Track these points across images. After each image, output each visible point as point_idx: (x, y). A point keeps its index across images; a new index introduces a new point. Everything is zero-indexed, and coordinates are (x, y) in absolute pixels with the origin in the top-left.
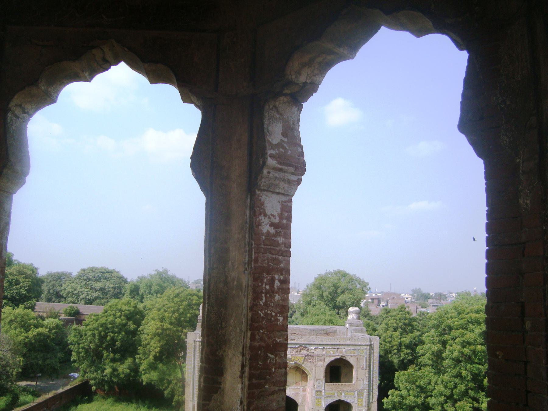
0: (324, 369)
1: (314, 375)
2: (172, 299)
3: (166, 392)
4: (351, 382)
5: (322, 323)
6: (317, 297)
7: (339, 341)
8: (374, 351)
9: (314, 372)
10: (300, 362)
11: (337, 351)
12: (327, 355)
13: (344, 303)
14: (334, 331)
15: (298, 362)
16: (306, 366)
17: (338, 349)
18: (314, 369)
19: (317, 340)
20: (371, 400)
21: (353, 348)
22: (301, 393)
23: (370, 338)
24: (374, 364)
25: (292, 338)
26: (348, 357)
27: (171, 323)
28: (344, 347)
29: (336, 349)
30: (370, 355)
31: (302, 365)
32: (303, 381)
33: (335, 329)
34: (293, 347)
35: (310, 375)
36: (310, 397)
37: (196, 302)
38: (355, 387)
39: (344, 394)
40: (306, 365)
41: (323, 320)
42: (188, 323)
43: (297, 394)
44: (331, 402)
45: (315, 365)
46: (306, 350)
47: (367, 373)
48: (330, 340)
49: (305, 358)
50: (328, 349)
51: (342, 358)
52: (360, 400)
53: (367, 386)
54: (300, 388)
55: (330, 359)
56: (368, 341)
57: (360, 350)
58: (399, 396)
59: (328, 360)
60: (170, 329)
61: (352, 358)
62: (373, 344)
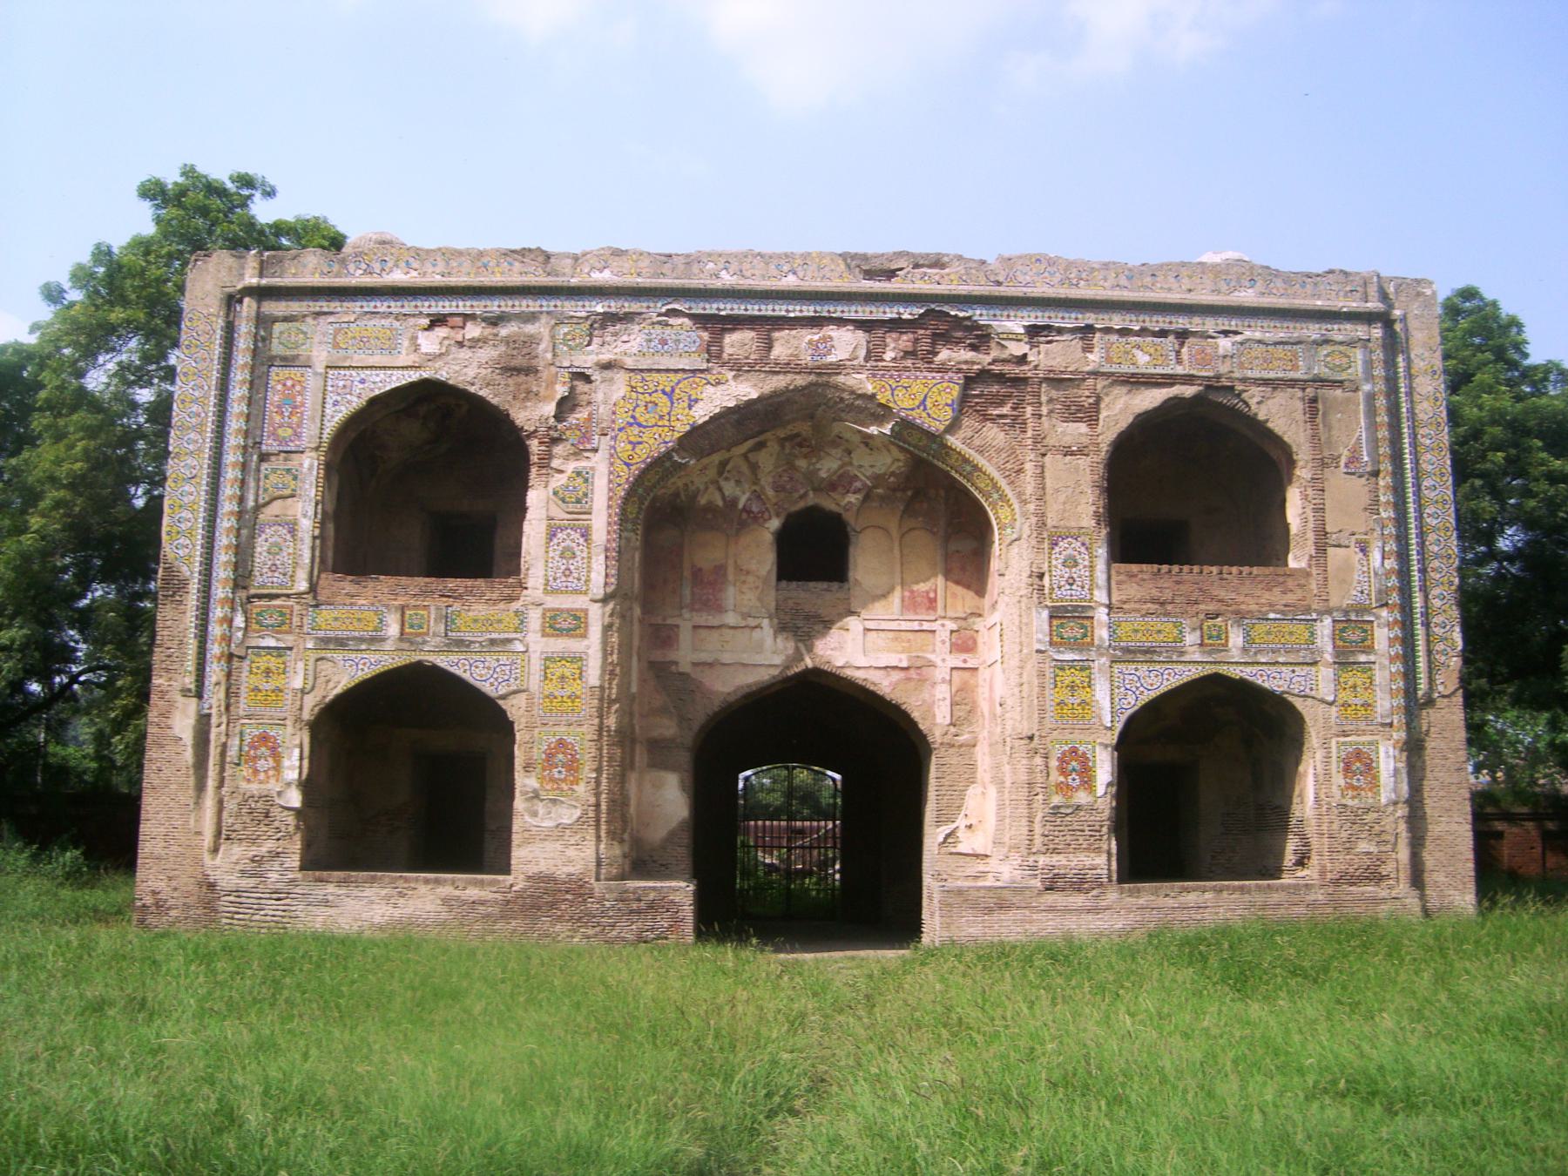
0: (1101, 469)
1: (1031, 507)
8: (1408, 361)
10: (936, 418)
11: (1178, 353)
12: (1113, 374)
17: (1182, 335)
18: (1029, 466)
20: (1423, 686)
21: (1281, 335)
22: (943, 660)
26: (1254, 390)
29: (1171, 338)
31: (953, 441)
34: (882, 323)
35: (1004, 513)
36: (1015, 662)
38: (1313, 586)
43: (917, 670)
44: (1163, 689)
45: (1038, 440)
47: (1385, 497)
48: (1129, 278)
49: (964, 398)
50: (1114, 338)
51: (1213, 397)
52: (1352, 678)
53: (1394, 581)
54: (935, 626)
56: (1373, 291)
61: (1281, 398)
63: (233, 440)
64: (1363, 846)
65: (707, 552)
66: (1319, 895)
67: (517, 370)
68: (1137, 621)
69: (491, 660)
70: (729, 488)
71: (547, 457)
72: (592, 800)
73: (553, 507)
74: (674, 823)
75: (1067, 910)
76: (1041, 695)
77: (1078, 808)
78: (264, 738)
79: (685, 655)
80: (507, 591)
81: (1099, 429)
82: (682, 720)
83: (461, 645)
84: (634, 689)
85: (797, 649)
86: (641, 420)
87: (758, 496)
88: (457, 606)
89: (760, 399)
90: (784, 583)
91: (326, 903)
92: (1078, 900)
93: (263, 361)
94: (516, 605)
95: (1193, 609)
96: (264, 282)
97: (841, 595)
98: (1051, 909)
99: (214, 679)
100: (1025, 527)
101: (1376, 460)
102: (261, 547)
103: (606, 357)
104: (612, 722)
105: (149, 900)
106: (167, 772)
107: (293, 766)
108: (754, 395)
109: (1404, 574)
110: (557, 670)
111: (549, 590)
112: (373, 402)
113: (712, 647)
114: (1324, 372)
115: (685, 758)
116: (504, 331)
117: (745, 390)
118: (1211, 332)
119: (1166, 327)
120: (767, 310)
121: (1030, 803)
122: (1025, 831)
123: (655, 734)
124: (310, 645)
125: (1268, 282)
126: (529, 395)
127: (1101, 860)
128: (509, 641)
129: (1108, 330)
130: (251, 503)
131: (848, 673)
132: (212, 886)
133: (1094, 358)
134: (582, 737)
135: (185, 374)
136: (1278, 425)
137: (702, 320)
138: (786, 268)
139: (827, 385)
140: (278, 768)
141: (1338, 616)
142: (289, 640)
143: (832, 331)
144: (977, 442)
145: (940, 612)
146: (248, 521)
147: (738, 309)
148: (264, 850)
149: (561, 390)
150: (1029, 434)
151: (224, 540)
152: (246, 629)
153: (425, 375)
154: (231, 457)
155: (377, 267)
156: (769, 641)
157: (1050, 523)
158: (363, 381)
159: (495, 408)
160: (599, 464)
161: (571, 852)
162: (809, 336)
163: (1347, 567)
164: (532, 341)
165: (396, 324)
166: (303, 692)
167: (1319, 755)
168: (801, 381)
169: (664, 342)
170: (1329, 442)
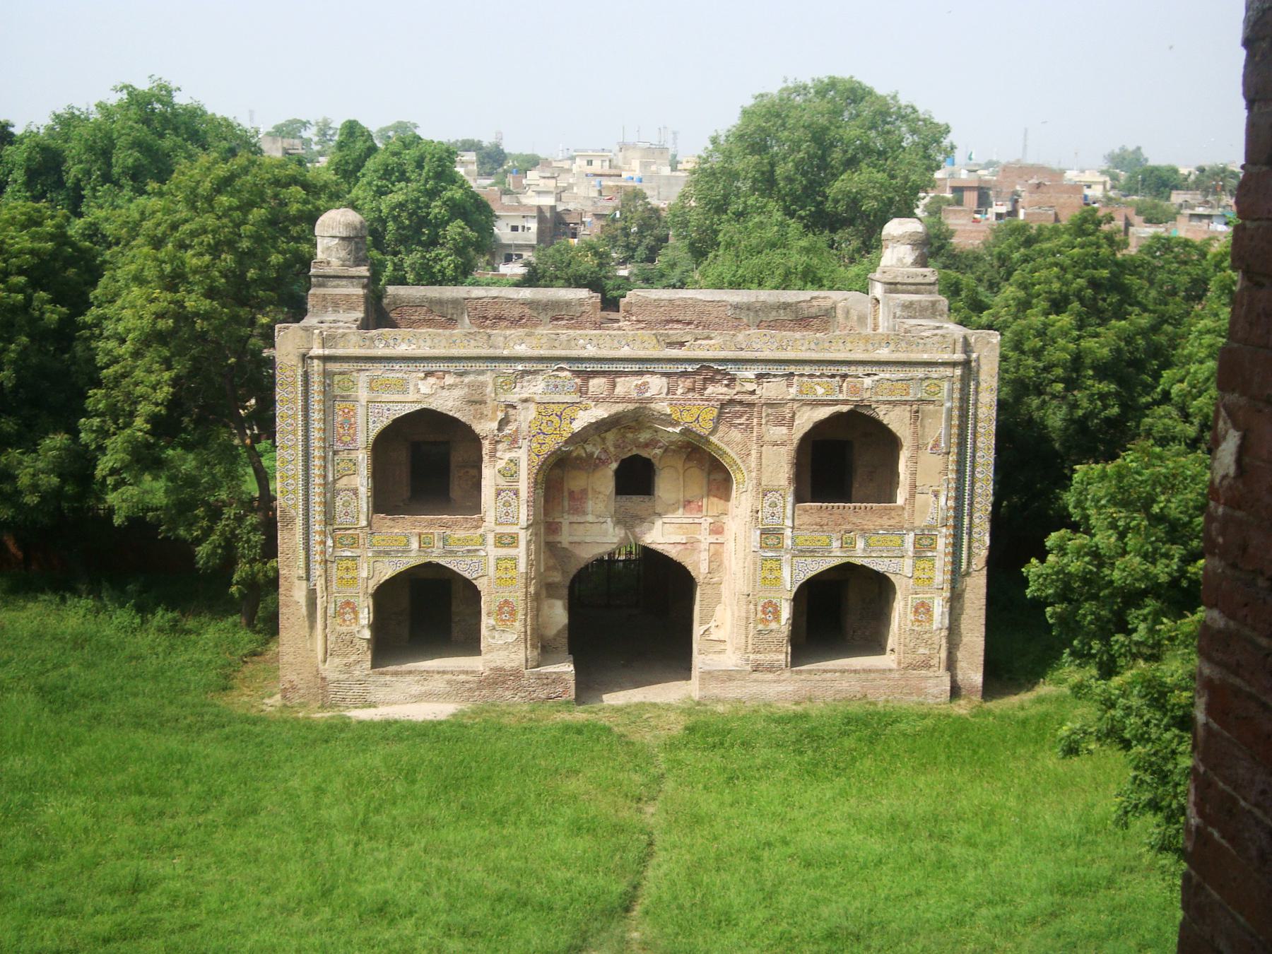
0: (793, 453)
1: (754, 474)
2: (209, 200)
3: (202, 550)
4: (891, 498)
5: (777, 280)
6: (749, 183)
7: (849, 346)
8: (978, 384)
9: (753, 465)
10: (703, 428)
11: (841, 387)
13: (854, 202)
14: (827, 310)
15: (696, 427)
16: (728, 442)
17: (844, 376)
18: (753, 452)
19: (764, 344)
20: (964, 566)
21: (901, 375)
22: (705, 538)
23: (965, 338)
24: (978, 435)
25: (674, 339)
26: (883, 407)
27: (211, 293)
28: (868, 370)
29: (838, 378)
30: (964, 399)
31: (712, 439)
32: (715, 496)
33: (828, 303)
34: (676, 373)
35: (739, 476)
36: (741, 555)
37: (299, 210)
39: (867, 544)
40: (726, 439)
41: (781, 271)
42: (272, 290)
43: (690, 545)
44: (819, 571)
45: (760, 438)
46: (726, 382)
47: (952, 467)
48: (817, 344)
49: (720, 414)
50: (805, 379)
52: (921, 564)
53: (951, 513)
55: (815, 415)
56: (959, 347)
57: (925, 383)
58: (1087, 554)
59: (807, 419)
60: (206, 316)
61: (898, 410)
62: (978, 358)
63: (316, 443)
64: (921, 651)
65: (577, 482)
66: (896, 675)
67: (475, 402)
68: (807, 535)
69: (468, 560)
70: (589, 448)
71: (494, 451)
72: (523, 630)
73: (498, 478)
74: (560, 626)
75: (763, 681)
76: (754, 574)
77: (771, 631)
78: (348, 603)
79: (565, 538)
80: (475, 523)
81: (793, 431)
82: (564, 572)
83: (452, 553)
84: (542, 570)
85: (626, 534)
86: (545, 431)
87: (605, 451)
88: (448, 532)
89: (610, 416)
90: (619, 497)
91: (386, 685)
92: (770, 676)
93: (329, 398)
94: (481, 531)
95: (838, 529)
96: (327, 352)
97: (650, 504)
98: (755, 681)
99: (318, 573)
100: (751, 485)
101: (949, 446)
102: (339, 503)
103: (525, 396)
104: (532, 589)
105: (288, 686)
106: (292, 620)
107: (365, 616)
108: (606, 416)
109: (958, 509)
110: (503, 564)
111: (498, 523)
112: (396, 421)
113: (579, 534)
114: (925, 396)
115: (565, 592)
116: (467, 380)
117: (600, 413)
118: (860, 375)
119: (835, 372)
120: (613, 367)
121: (747, 628)
122: (744, 641)
123: (550, 580)
124: (370, 555)
125: (897, 344)
126: (482, 416)
127: (782, 656)
128: (478, 550)
129: (802, 375)
130: (331, 479)
131: (653, 546)
132: (323, 679)
133: (793, 391)
134: (517, 596)
135: (282, 401)
136: (894, 427)
137: (577, 373)
138: (623, 343)
139: (645, 407)
140: (356, 618)
141: (918, 532)
142: (358, 552)
143: (647, 378)
144: (726, 439)
145: (704, 513)
146: (330, 491)
147: (597, 367)
148: (351, 660)
149: (501, 415)
150: (755, 434)
151: (316, 499)
152: (334, 547)
153: (424, 406)
154: (317, 453)
155: (392, 342)
156: (611, 530)
157: (763, 483)
158: (389, 410)
159: (464, 424)
160: (522, 455)
161: (512, 656)
162: (637, 381)
163: (927, 505)
164: (483, 385)
165: (405, 376)
166: (368, 578)
167: (902, 603)
168: (631, 407)
169: (556, 387)
170: (923, 435)
